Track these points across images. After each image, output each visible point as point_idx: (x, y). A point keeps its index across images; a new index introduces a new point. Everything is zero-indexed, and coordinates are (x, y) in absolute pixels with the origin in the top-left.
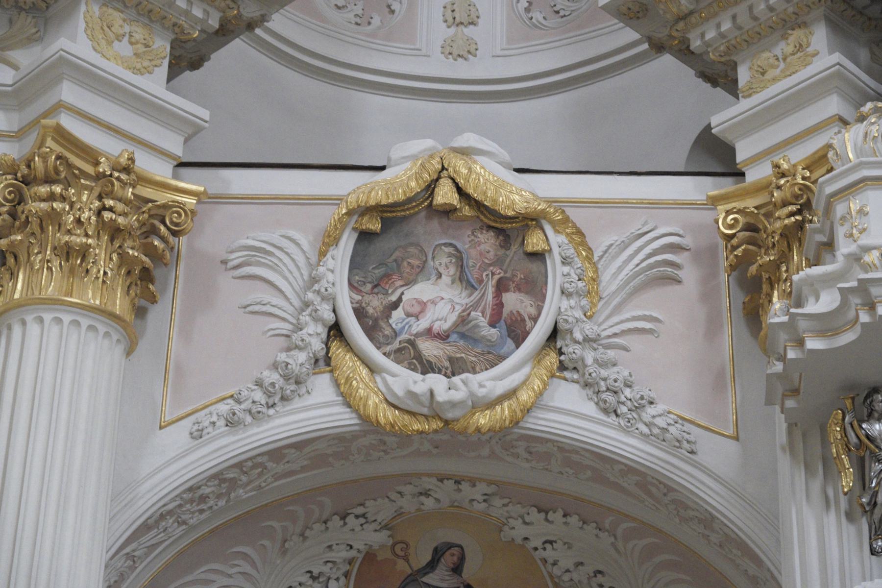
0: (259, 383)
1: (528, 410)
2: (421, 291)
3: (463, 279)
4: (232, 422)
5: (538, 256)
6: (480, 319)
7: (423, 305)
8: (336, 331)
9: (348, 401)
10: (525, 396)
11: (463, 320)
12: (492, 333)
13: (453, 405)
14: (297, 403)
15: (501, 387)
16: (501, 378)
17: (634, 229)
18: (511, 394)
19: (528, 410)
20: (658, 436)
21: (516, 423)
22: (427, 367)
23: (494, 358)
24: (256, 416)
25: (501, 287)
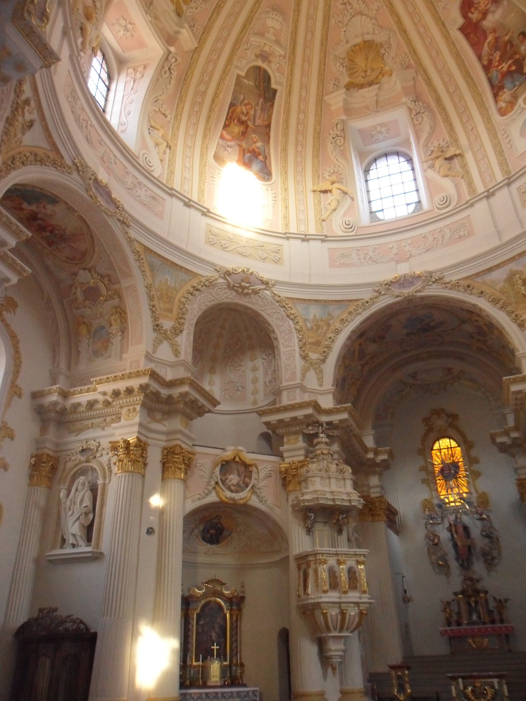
0: (204, 492)
1: (248, 501)
2: (231, 476)
3: (239, 475)
4: (199, 499)
5: (251, 472)
6: (241, 483)
7: (232, 479)
8: (217, 483)
9: (218, 496)
10: (248, 498)
11: (238, 483)
12: (243, 485)
13: (237, 500)
14: (210, 496)
15: (245, 496)
16: (244, 494)
17: (264, 466)
18: (246, 498)
19: (248, 501)
20: (269, 507)
21: (246, 502)
22: (232, 491)
23: (243, 490)
24: (203, 498)
25: (245, 477)
